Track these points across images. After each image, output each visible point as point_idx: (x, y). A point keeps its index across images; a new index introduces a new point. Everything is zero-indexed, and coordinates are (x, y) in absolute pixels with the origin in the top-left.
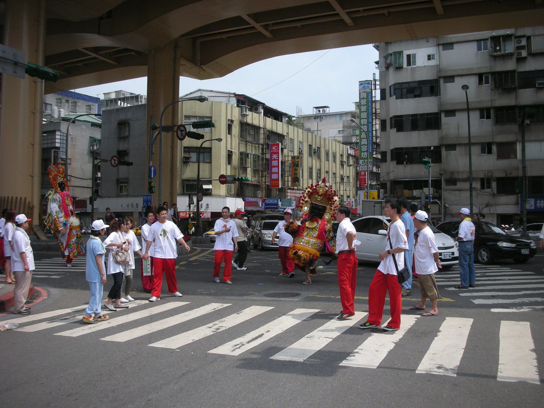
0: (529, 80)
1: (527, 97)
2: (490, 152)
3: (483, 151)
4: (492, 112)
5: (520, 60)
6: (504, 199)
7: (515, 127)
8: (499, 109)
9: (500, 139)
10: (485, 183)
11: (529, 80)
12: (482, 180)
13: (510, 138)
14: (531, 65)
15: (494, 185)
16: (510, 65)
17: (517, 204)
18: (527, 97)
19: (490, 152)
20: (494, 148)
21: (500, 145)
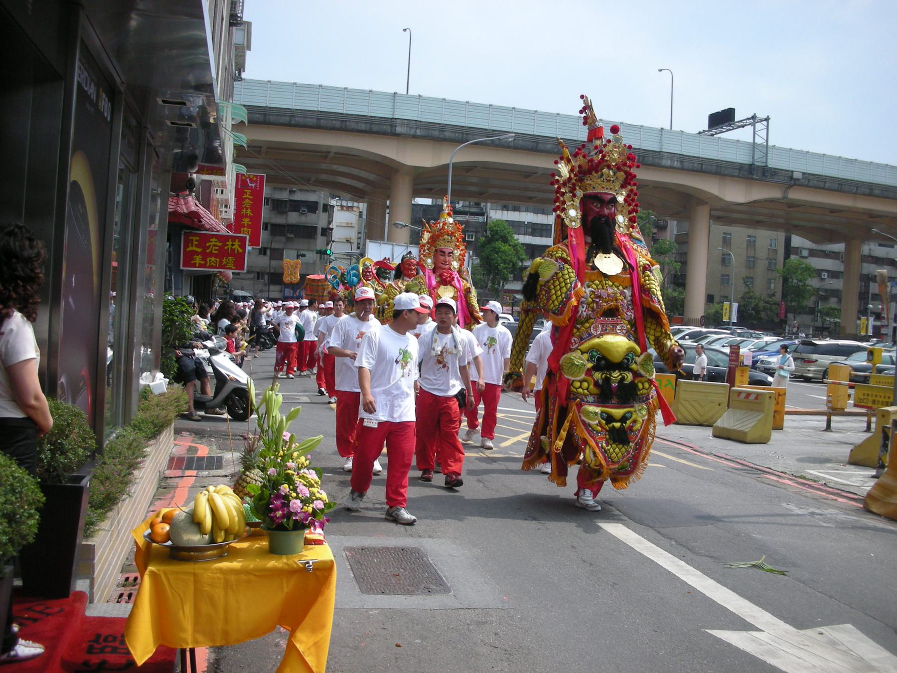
0: (296, 206)
1: (293, 218)
2: (265, 254)
3: (260, 253)
4: (269, 227)
5: (292, 192)
6: (272, 287)
7: (283, 239)
8: (274, 226)
9: (274, 246)
10: (259, 275)
11: (296, 206)
12: (258, 273)
13: (280, 246)
14: (298, 196)
15: (266, 277)
16: (284, 196)
17: (281, 291)
18: (293, 218)
19: (265, 254)
20: (268, 252)
21: (271, 249)
